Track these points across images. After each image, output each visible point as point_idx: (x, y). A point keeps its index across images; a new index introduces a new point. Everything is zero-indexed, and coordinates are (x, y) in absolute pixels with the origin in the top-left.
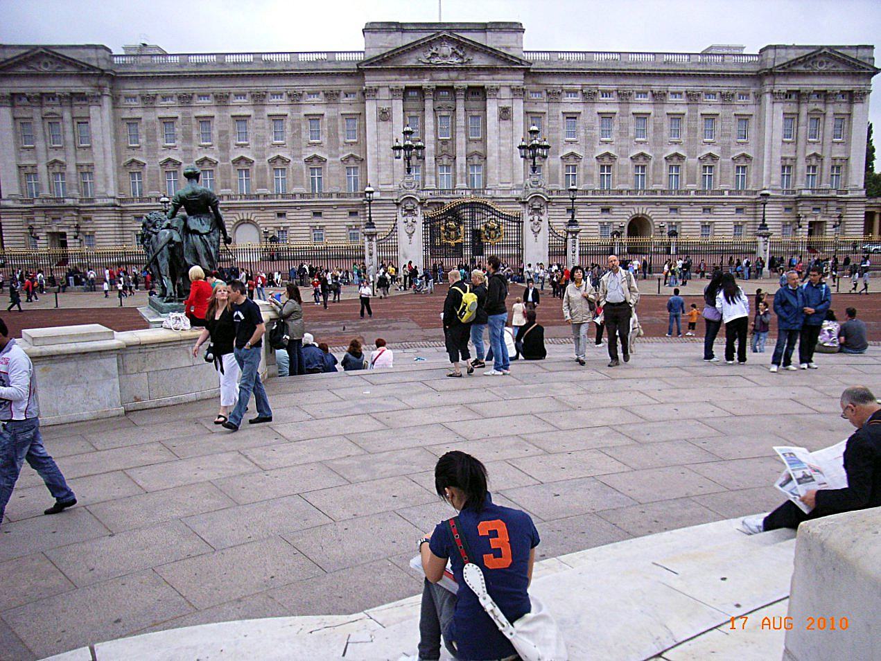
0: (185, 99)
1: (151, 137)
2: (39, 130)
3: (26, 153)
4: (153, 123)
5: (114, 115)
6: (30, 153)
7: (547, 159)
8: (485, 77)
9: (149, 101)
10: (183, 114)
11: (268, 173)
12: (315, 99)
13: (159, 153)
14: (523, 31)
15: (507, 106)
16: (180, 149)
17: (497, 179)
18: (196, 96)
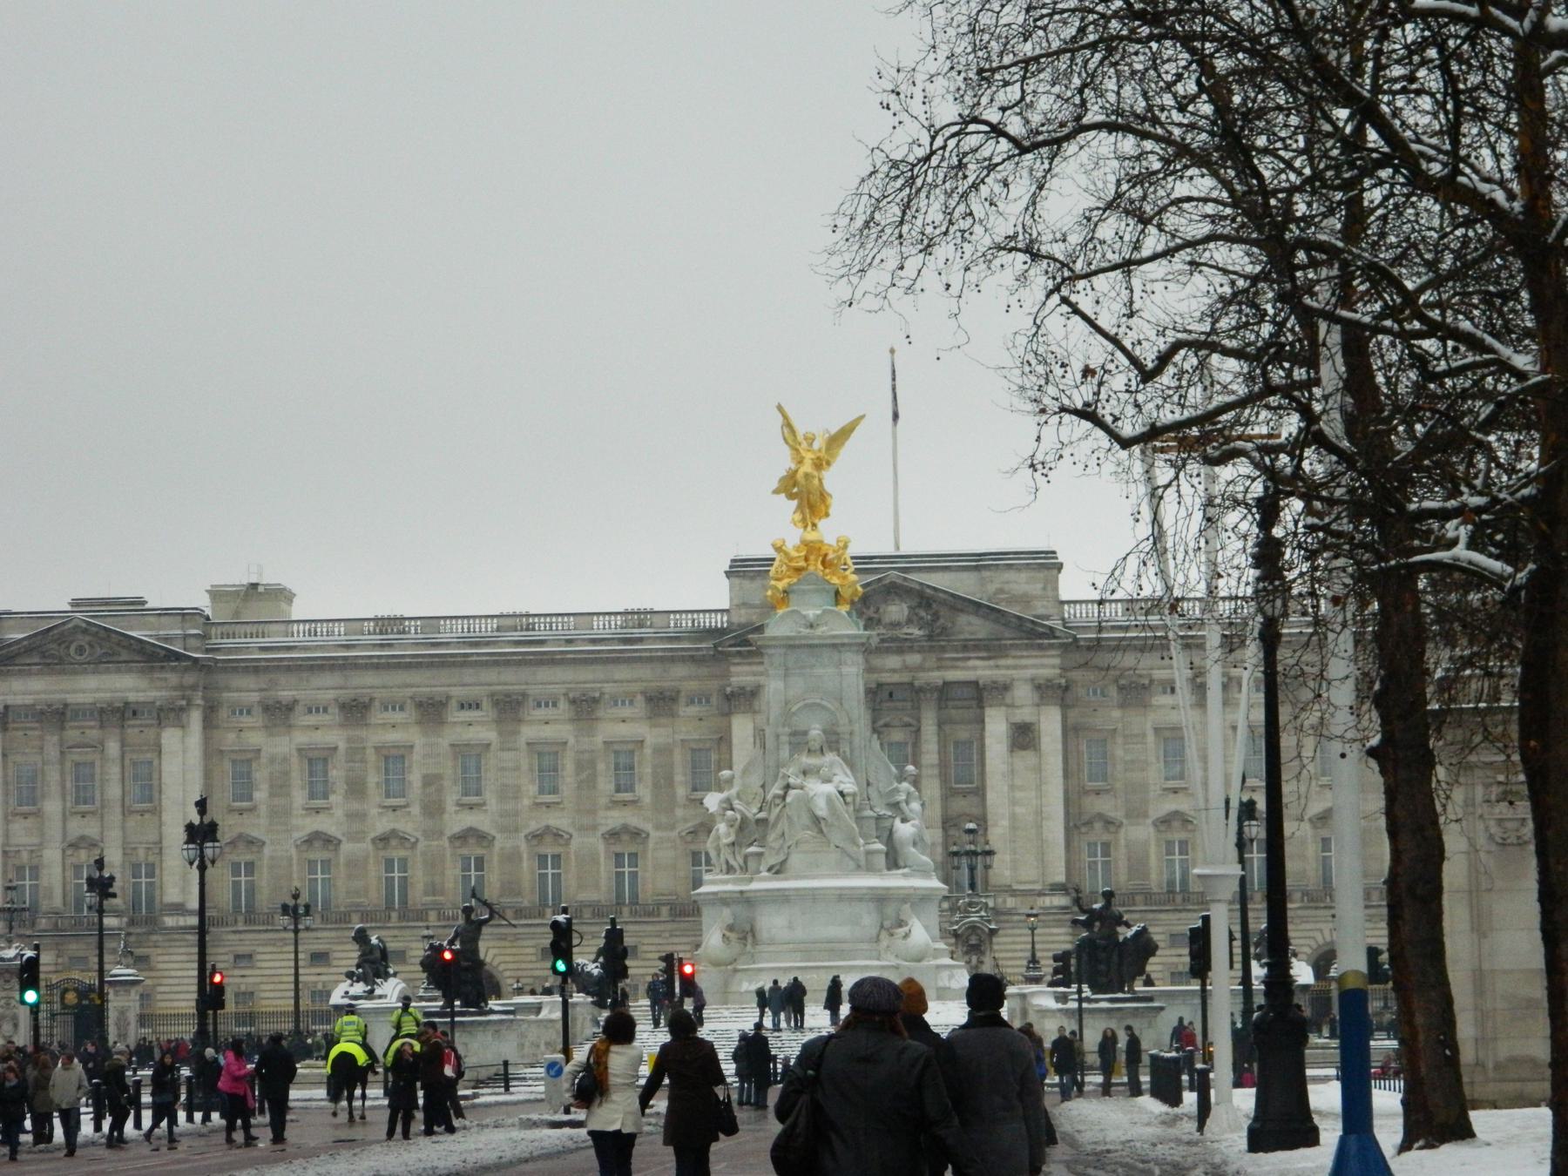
0: (355, 710)
1: (280, 787)
2: (53, 776)
3: (18, 826)
4: (285, 760)
5: (207, 740)
6: (30, 822)
7: (1123, 830)
8: (978, 663)
9: (279, 713)
10: (349, 740)
11: (525, 864)
12: (626, 712)
13: (294, 822)
14: (1060, 567)
15: (1028, 719)
16: (339, 813)
17: (1007, 873)
18: (377, 703)
